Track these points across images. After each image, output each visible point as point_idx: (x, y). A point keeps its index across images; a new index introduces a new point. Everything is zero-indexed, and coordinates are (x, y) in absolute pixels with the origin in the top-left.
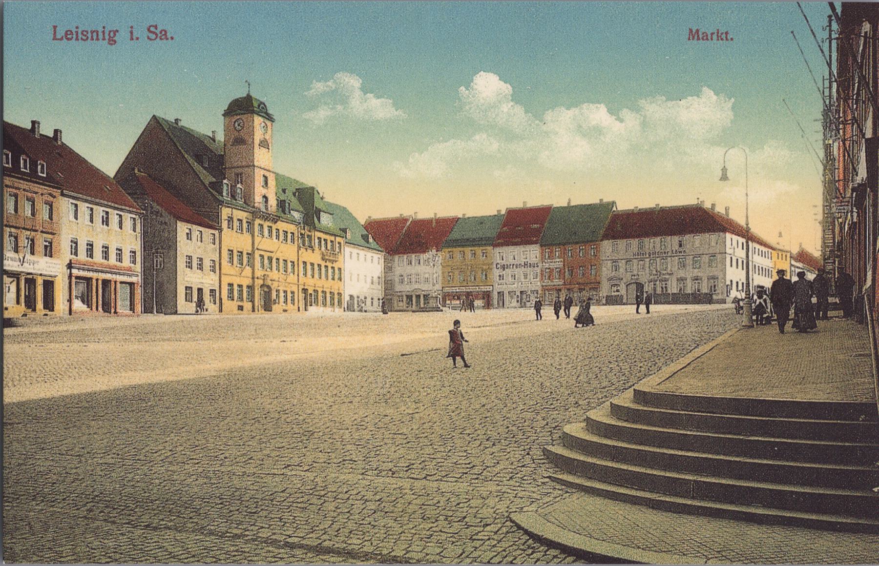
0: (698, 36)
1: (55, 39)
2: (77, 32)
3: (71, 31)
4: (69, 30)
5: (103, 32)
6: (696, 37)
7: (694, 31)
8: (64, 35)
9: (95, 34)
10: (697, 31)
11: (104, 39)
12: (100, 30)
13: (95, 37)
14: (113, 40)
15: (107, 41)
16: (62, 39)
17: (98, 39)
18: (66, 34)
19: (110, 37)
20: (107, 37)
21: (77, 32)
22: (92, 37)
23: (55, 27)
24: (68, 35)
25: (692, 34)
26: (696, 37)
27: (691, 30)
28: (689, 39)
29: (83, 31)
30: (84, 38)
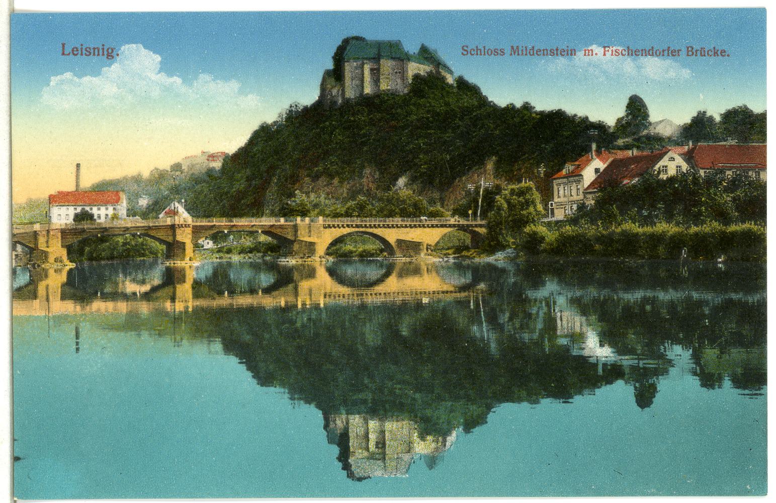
0: (518, 53)
1: (63, 54)
2: (82, 49)
3: (77, 48)
4: (73, 49)
5: (103, 49)
6: (517, 53)
7: (515, 48)
8: (71, 51)
9: (96, 50)
10: (518, 47)
11: (103, 55)
12: (101, 47)
13: (96, 53)
14: (110, 56)
15: (106, 56)
16: (69, 54)
17: (98, 55)
18: (73, 50)
19: (108, 53)
20: (106, 53)
21: (82, 49)
22: (94, 52)
23: (63, 45)
24: (75, 52)
25: (513, 49)
26: (517, 53)
27: (512, 47)
28: (511, 54)
29: (86, 48)
30: (88, 53)
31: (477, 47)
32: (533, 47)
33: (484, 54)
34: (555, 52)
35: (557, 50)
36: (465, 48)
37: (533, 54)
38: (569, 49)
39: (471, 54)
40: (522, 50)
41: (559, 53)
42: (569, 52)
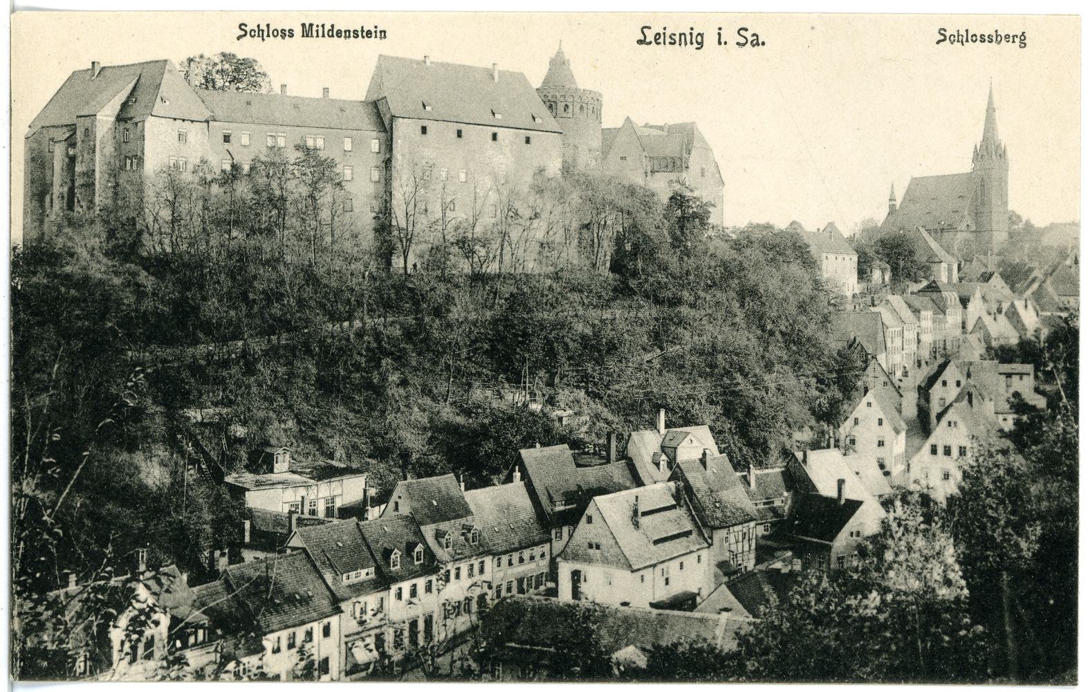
2: (376, 32)
10: (311, 25)
21: (376, 32)
31: (258, 26)
32: (332, 26)
33: (323, 36)
34: (360, 33)
35: (362, 31)
36: (243, 27)
37: (333, 36)
38: (378, 30)
39: (252, 37)
40: (317, 31)
41: (364, 34)
42: (378, 34)
